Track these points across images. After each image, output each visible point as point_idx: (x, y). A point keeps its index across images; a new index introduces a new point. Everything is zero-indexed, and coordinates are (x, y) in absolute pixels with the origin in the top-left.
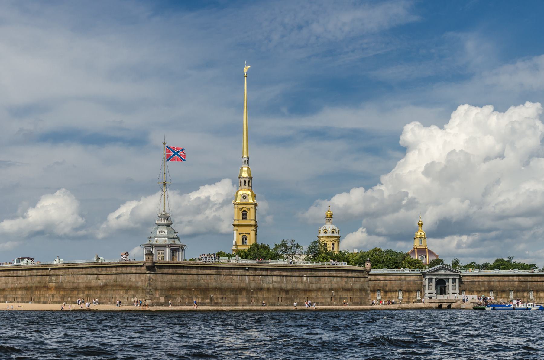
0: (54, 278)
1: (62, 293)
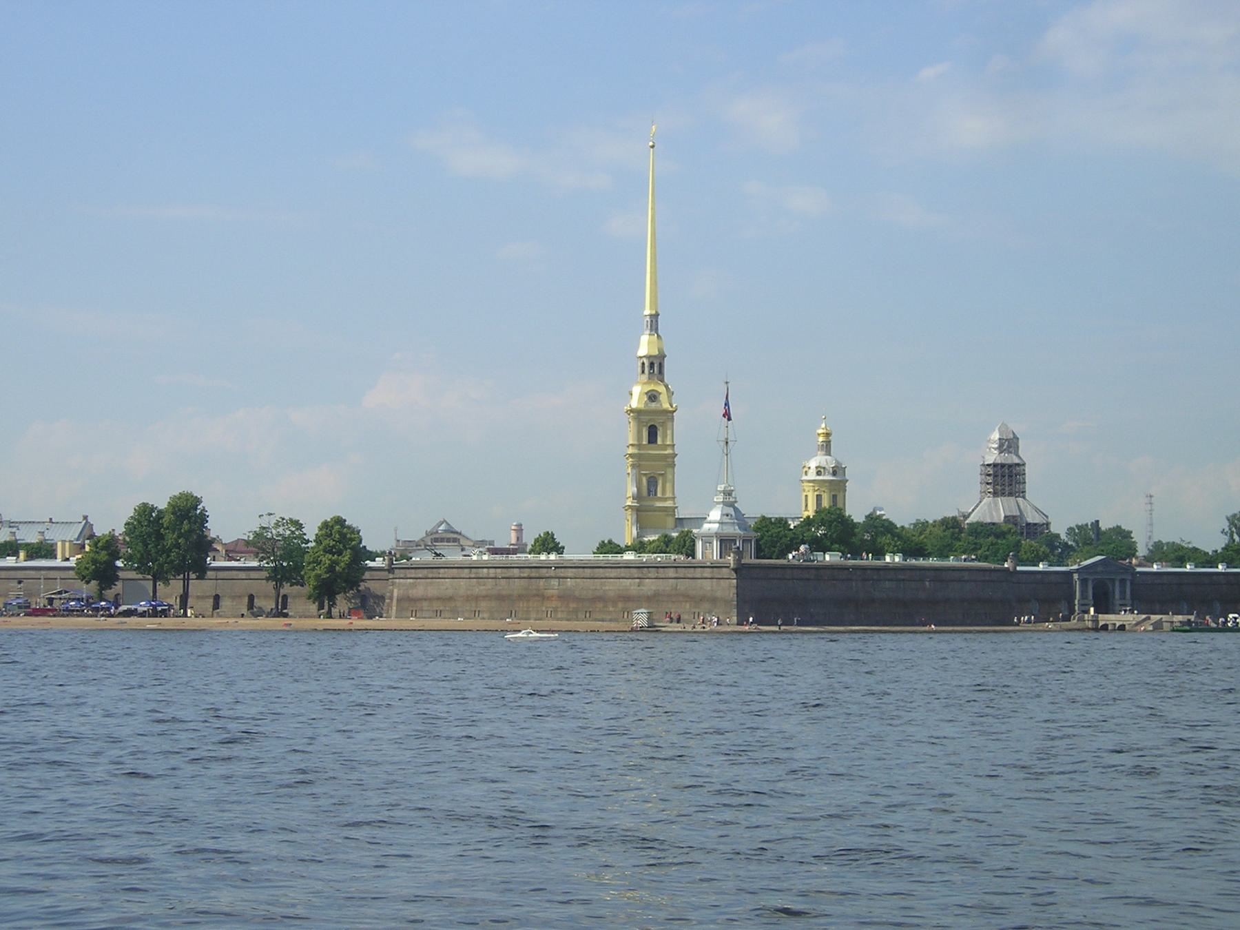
0: (555, 582)
1: (573, 605)
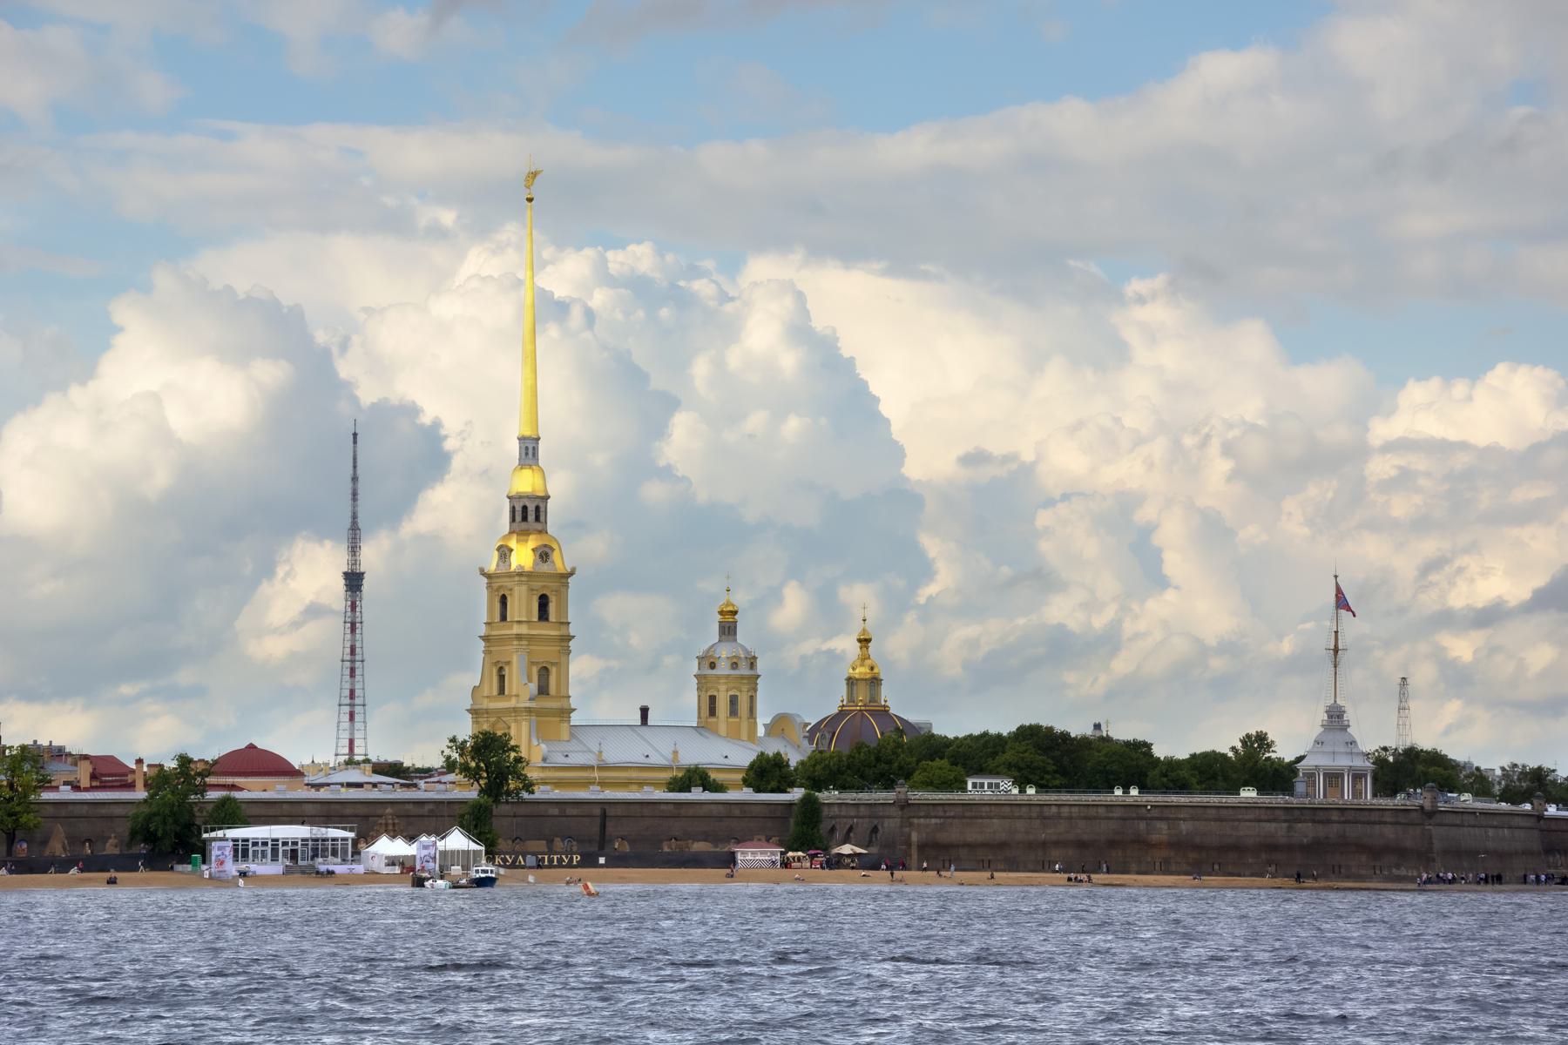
0: (1163, 826)
1: (1192, 855)
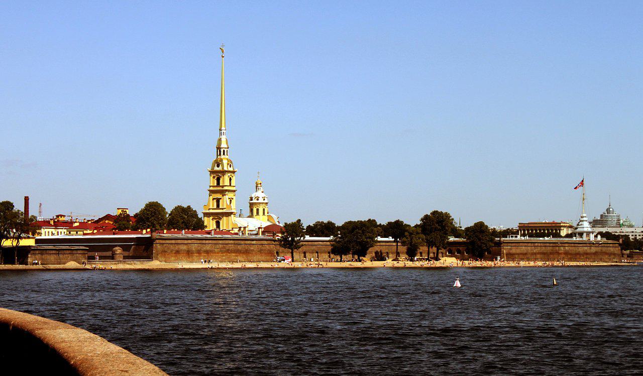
0: (562, 248)
